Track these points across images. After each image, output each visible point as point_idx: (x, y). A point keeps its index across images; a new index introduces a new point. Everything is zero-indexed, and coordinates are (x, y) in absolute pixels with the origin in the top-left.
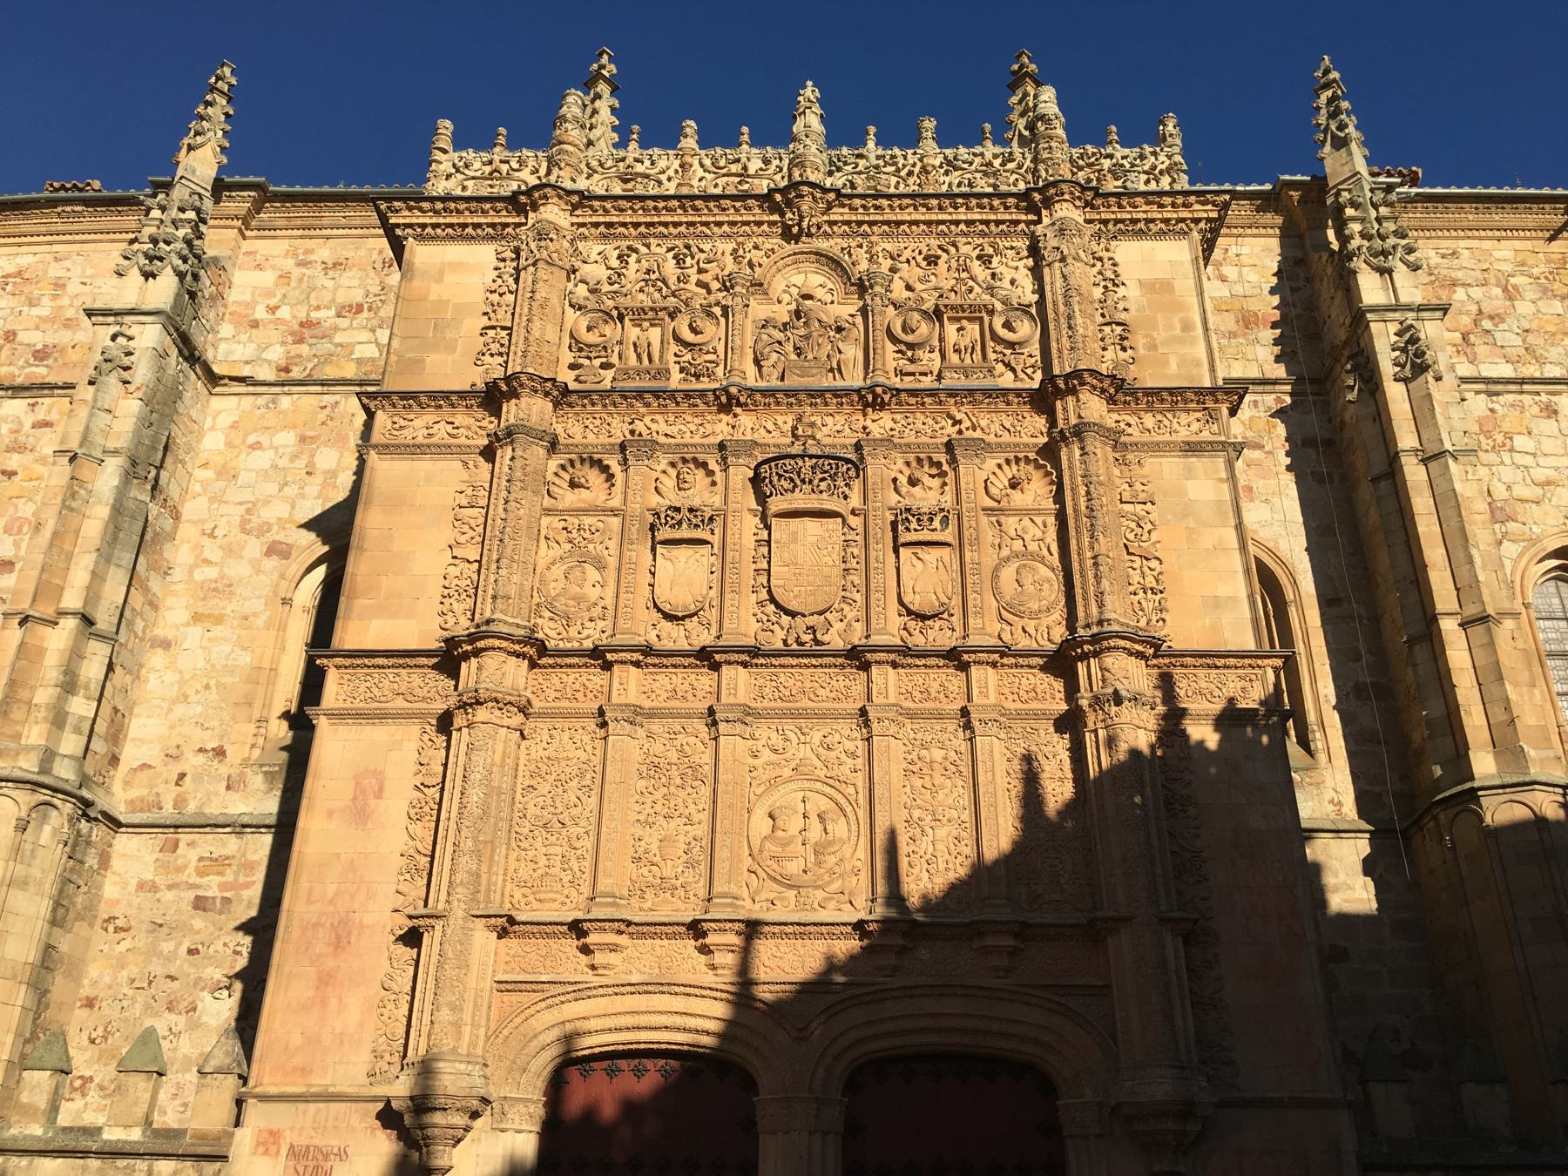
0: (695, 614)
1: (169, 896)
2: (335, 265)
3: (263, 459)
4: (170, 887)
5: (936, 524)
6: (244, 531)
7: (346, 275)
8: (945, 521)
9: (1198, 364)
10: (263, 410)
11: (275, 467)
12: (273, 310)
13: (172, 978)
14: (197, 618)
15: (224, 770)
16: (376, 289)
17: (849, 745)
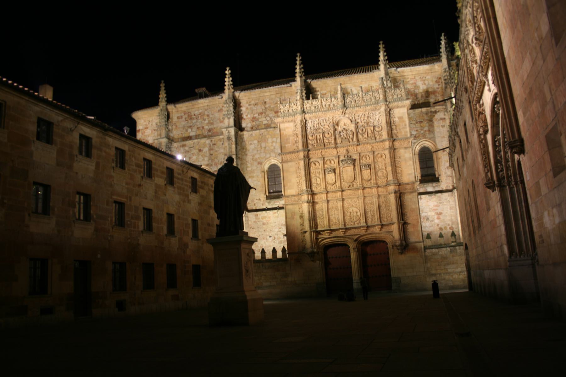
0: (334, 185)
1: (259, 223)
2: (256, 104)
3: (252, 147)
4: (258, 222)
5: (367, 167)
6: (253, 160)
7: (258, 106)
8: (368, 166)
9: (407, 132)
10: (250, 137)
11: (255, 148)
12: (247, 116)
13: (262, 235)
14: (250, 177)
15: (261, 202)
16: (263, 108)
17: (357, 202)
